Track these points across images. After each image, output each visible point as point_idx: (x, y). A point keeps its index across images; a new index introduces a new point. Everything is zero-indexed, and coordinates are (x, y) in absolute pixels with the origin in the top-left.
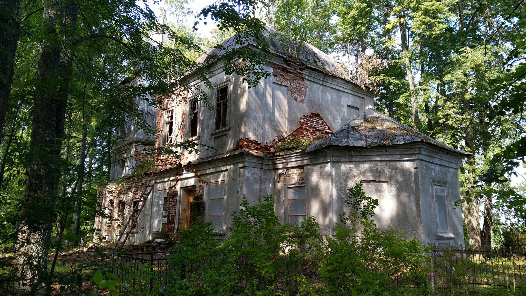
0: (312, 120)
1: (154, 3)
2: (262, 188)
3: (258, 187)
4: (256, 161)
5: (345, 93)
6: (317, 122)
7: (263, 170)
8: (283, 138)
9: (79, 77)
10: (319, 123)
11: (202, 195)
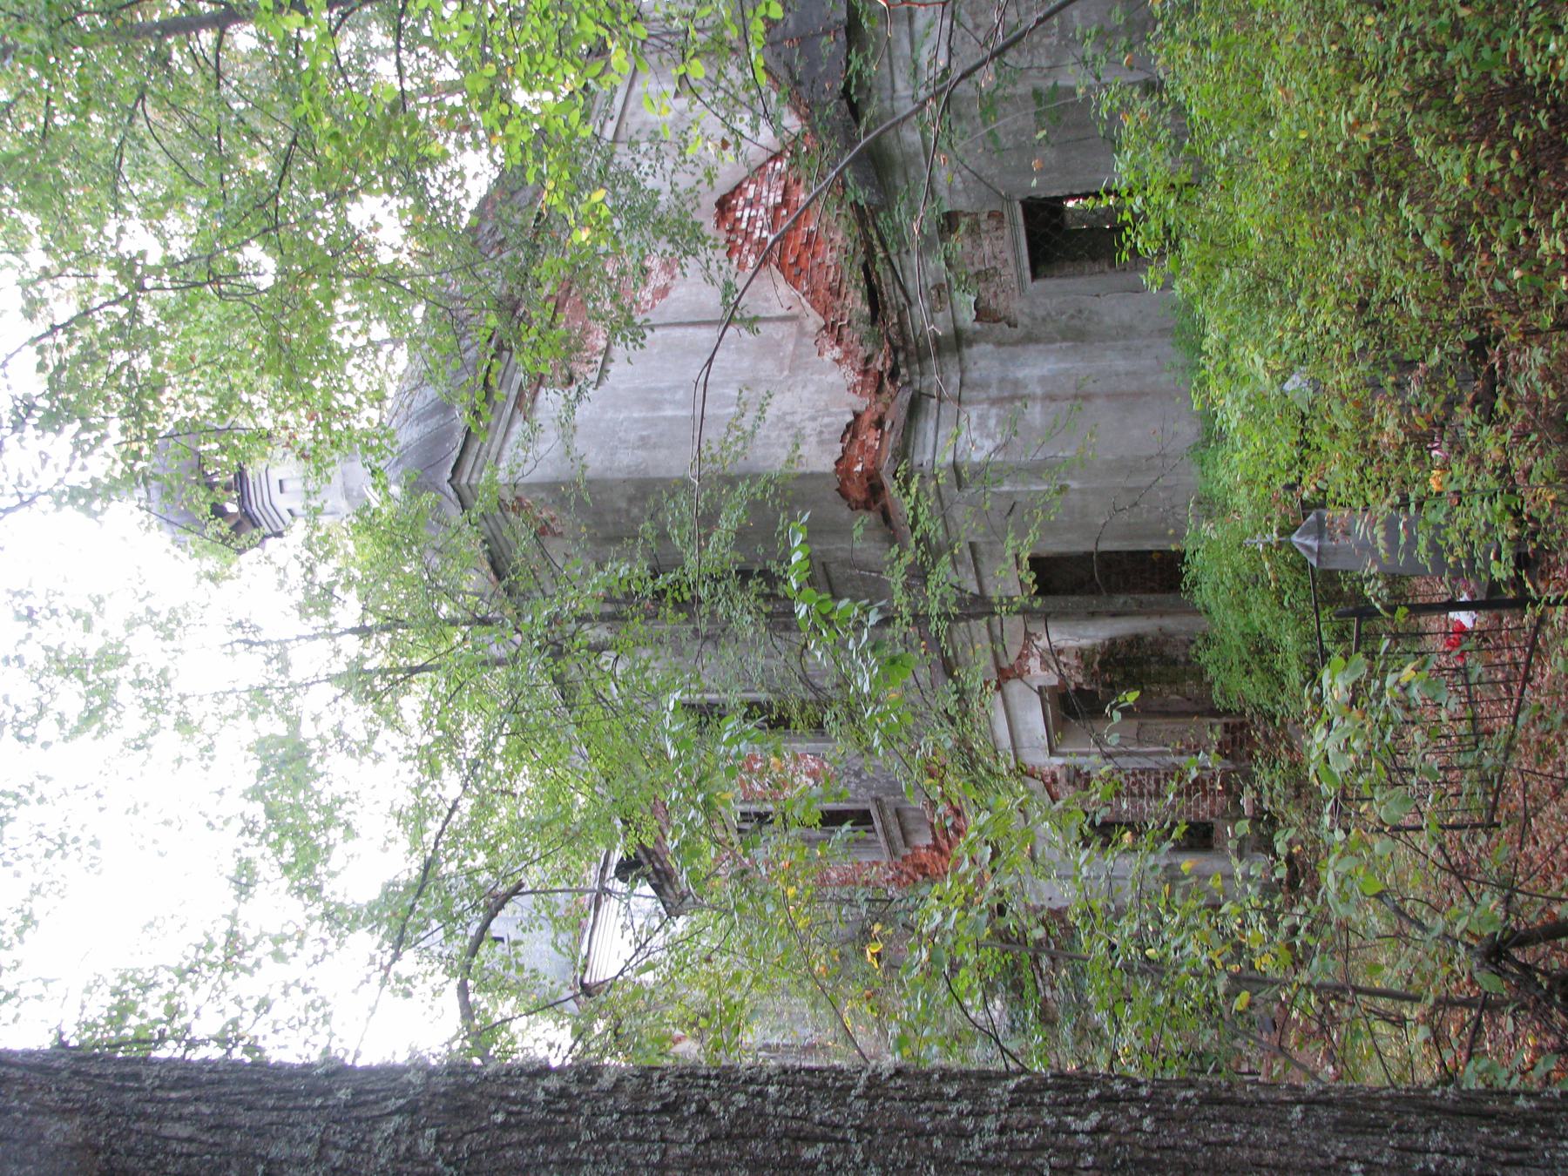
0: (744, 225)
1: (8, 591)
2: (1039, 391)
3: (1038, 408)
4: (931, 424)
5: (628, 112)
6: (751, 204)
7: (965, 395)
8: (825, 327)
9: (494, 792)
10: (758, 196)
11: (1081, 654)
